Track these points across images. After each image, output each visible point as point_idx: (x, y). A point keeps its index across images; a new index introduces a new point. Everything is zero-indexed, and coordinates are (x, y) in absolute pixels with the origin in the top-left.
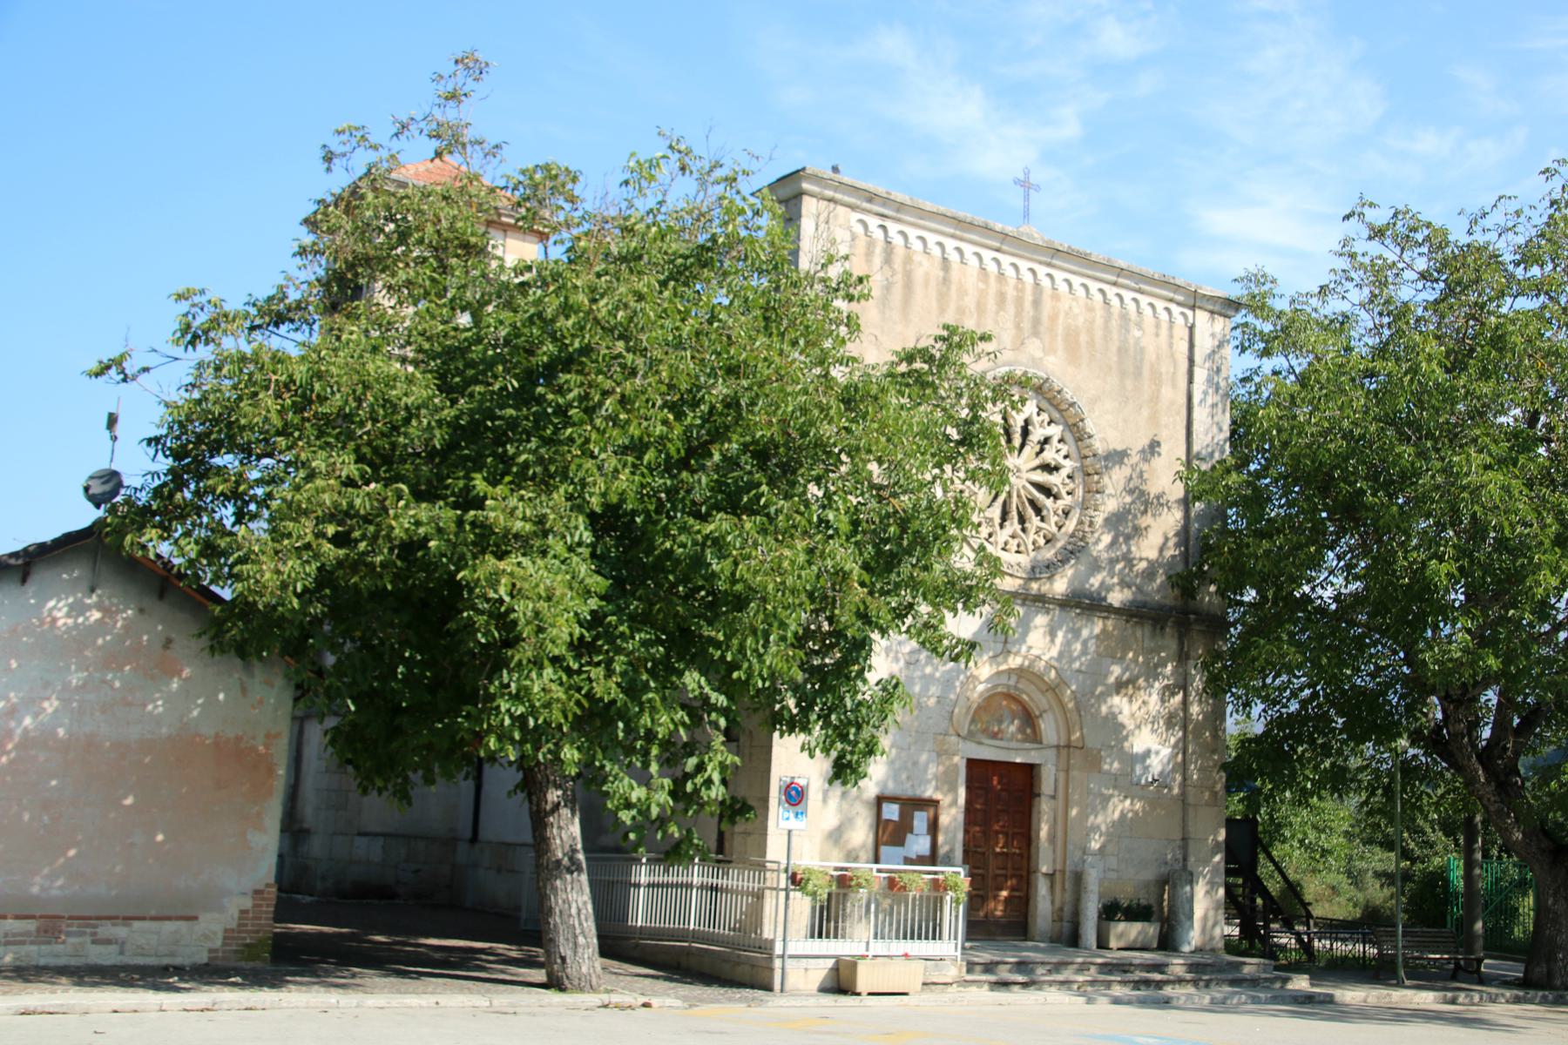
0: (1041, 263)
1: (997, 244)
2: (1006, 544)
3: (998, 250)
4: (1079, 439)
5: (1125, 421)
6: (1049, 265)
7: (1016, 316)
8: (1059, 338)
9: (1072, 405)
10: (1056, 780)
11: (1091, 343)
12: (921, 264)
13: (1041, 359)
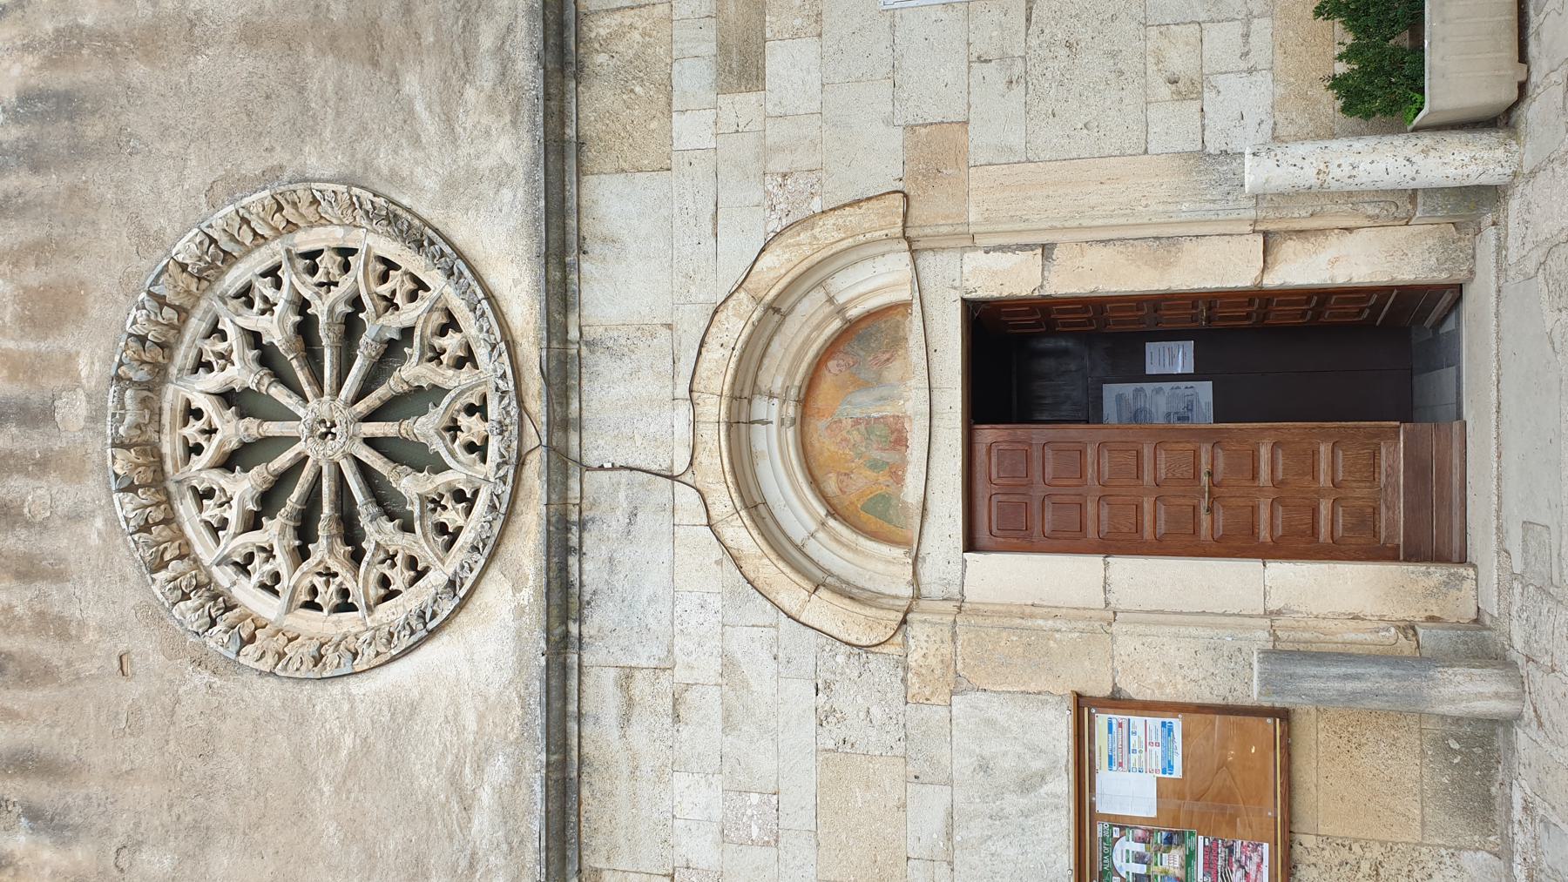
2: (470, 447)
5: (164, 132)
8: (43, 346)
10: (1002, 248)
11: (39, 251)
13: (89, 396)
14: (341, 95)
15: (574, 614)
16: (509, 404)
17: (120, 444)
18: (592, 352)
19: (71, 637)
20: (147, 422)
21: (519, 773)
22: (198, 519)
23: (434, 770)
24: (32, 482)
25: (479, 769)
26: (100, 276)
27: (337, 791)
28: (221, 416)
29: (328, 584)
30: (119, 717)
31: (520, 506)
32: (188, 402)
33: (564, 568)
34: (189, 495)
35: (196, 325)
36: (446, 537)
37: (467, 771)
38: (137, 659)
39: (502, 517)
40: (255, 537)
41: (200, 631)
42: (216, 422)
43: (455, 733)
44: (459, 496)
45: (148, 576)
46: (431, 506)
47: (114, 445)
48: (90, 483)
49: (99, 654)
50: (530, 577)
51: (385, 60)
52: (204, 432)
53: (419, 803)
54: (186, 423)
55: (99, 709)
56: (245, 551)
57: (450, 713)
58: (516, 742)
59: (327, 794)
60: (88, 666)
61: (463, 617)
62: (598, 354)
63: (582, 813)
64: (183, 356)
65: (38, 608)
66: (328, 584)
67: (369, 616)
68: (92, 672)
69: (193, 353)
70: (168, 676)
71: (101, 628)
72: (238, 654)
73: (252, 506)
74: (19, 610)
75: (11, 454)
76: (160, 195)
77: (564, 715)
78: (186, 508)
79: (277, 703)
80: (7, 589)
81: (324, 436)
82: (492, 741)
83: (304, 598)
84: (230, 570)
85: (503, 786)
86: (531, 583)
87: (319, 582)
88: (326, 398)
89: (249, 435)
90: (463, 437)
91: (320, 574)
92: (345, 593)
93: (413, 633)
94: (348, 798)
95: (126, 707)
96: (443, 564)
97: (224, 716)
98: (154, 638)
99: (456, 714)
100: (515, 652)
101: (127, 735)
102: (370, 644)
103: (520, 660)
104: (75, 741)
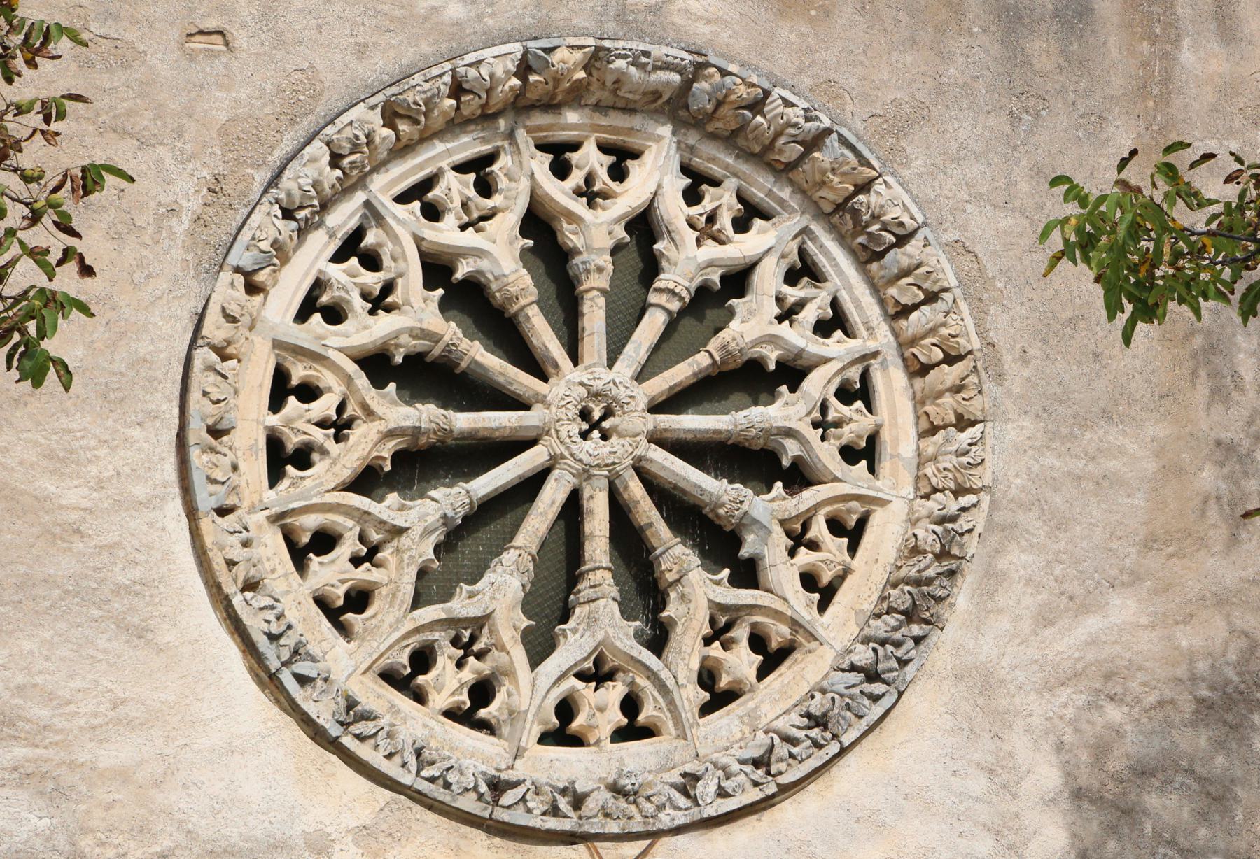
4: (867, 256)
9: (815, 142)
14: (1107, 483)
26: (837, 47)
30: (110, 22)
35: (762, 186)
39: (486, 814)
43: (94, 722)
51: (1153, 561)
54: (604, 148)
57: (131, 710)
64: (715, 158)
69: (716, 170)
76: (956, 160)
89: (588, 271)
93: (273, 638)
95: (129, 36)
100: (247, 840)
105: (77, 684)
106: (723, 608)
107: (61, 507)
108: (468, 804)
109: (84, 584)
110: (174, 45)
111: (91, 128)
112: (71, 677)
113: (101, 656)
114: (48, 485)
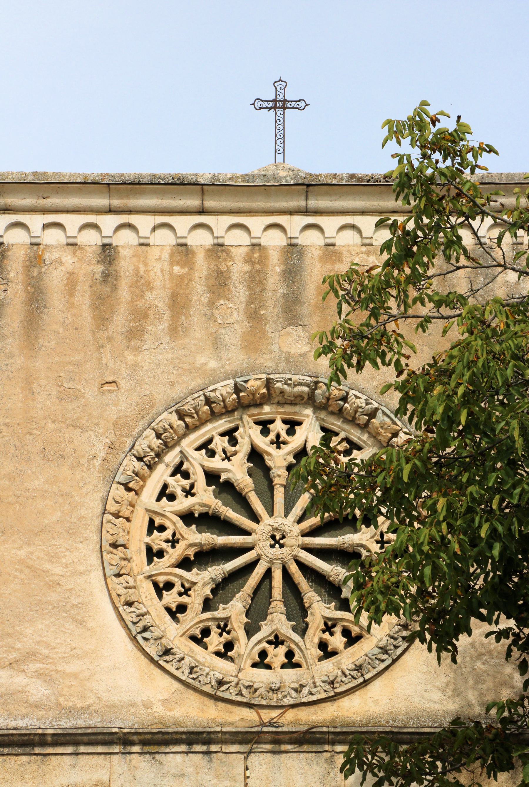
0: (291, 212)
1: (194, 202)
2: (263, 654)
3: (202, 212)
6: (306, 212)
7: (251, 300)
12: (59, 261)
15: (147, 749)
16: (292, 697)
17: (268, 383)
18: (326, 761)
19: (129, 341)
20: (286, 397)
21: (37, 706)
22: (214, 433)
23: (38, 639)
24: (242, 307)
25: (40, 675)
27: (21, 561)
28: (289, 454)
29: (167, 541)
31: (221, 705)
32: (300, 423)
33: (177, 742)
34: (232, 425)
36: (200, 636)
37: (38, 666)
38: (113, 396)
39: (214, 693)
40: (200, 479)
41: (135, 452)
42: (286, 449)
44: (229, 646)
45: (174, 408)
46: (222, 624)
47: (268, 380)
48: (242, 357)
49: (117, 364)
50: (172, 713)
52: (278, 436)
53: (13, 627)
55: (78, 364)
56: (191, 471)
57: (78, 651)
58: (59, 704)
59: (19, 553)
60: (109, 355)
61: (144, 661)
62: (325, 765)
63: (9, 757)
65: (151, 312)
66: (167, 541)
67: (145, 577)
68: (104, 359)
70: (102, 422)
71: (136, 365)
72: (119, 483)
73: (223, 477)
74: (149, 296)
75: (264, 289)
77: (77, 744)
78: (223, 424)
79: (83, 512)
80: (164, 286)
81: (273, 537)
82: (58, 685)
83: (158, 521)
84: (177, 460)
85: (27, 693)
86: (168, 713)
87: (167, 534)
88: (302, 540)
90: (270, 649)
91: (174, 535)
92: (160, 554)
93: (134, 623)
94: (16, 570)
96: (181, 636)
97: (72, 468)
98: (129, 410)
99: (77, 657)
100: (120, 702)
101: (58, 389)
102: (126, 588)
103: (114, 706)
104: (53, 343)
105: (58, 641)
106: (330, 619)
107: (52, 574)
108: (207, 689)
109: (60, 604)
110: (96, 389)
111: (64, 425)
112: (56, 638)
113: (67, 631)
114: (47, 566)
